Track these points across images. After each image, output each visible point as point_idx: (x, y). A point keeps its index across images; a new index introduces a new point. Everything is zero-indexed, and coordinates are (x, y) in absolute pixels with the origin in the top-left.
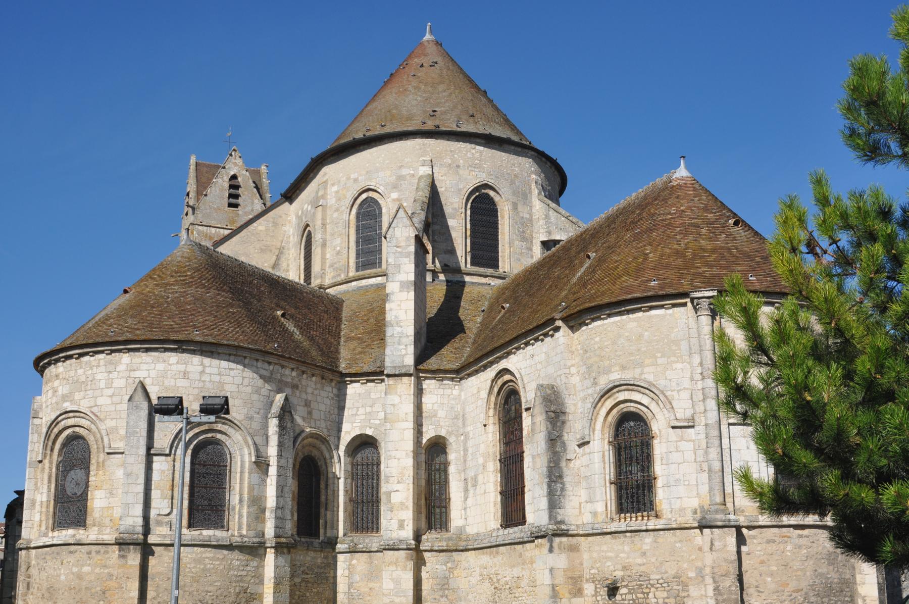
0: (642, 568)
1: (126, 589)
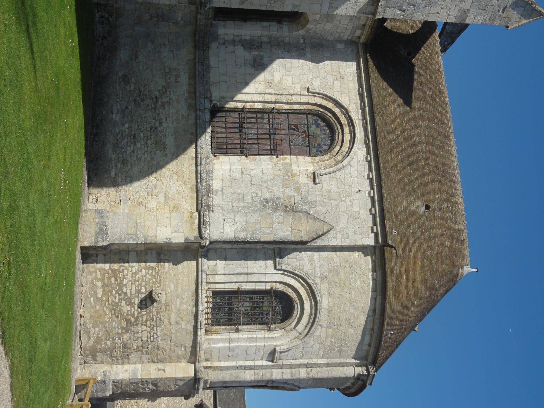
0: (166, 321)
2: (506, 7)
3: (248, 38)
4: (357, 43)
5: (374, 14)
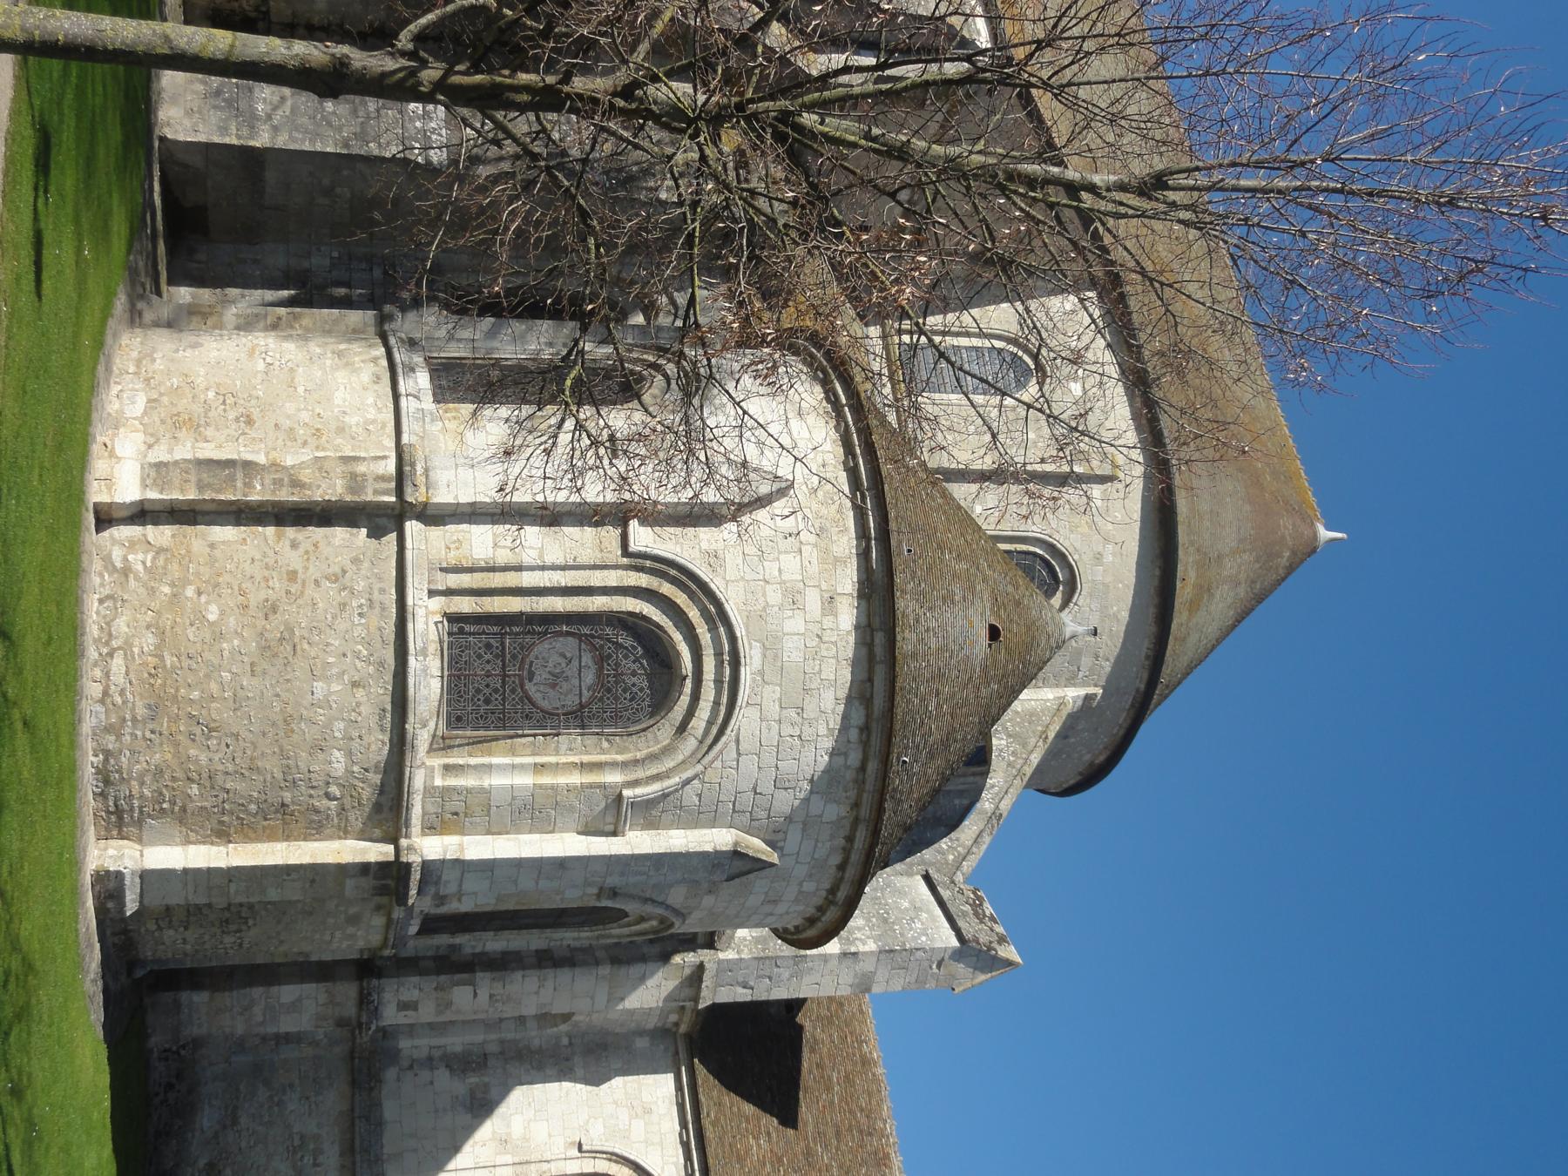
2: (943, 959)
3: (458, 1049)
4: (675, 1033)
5: (696, 999)
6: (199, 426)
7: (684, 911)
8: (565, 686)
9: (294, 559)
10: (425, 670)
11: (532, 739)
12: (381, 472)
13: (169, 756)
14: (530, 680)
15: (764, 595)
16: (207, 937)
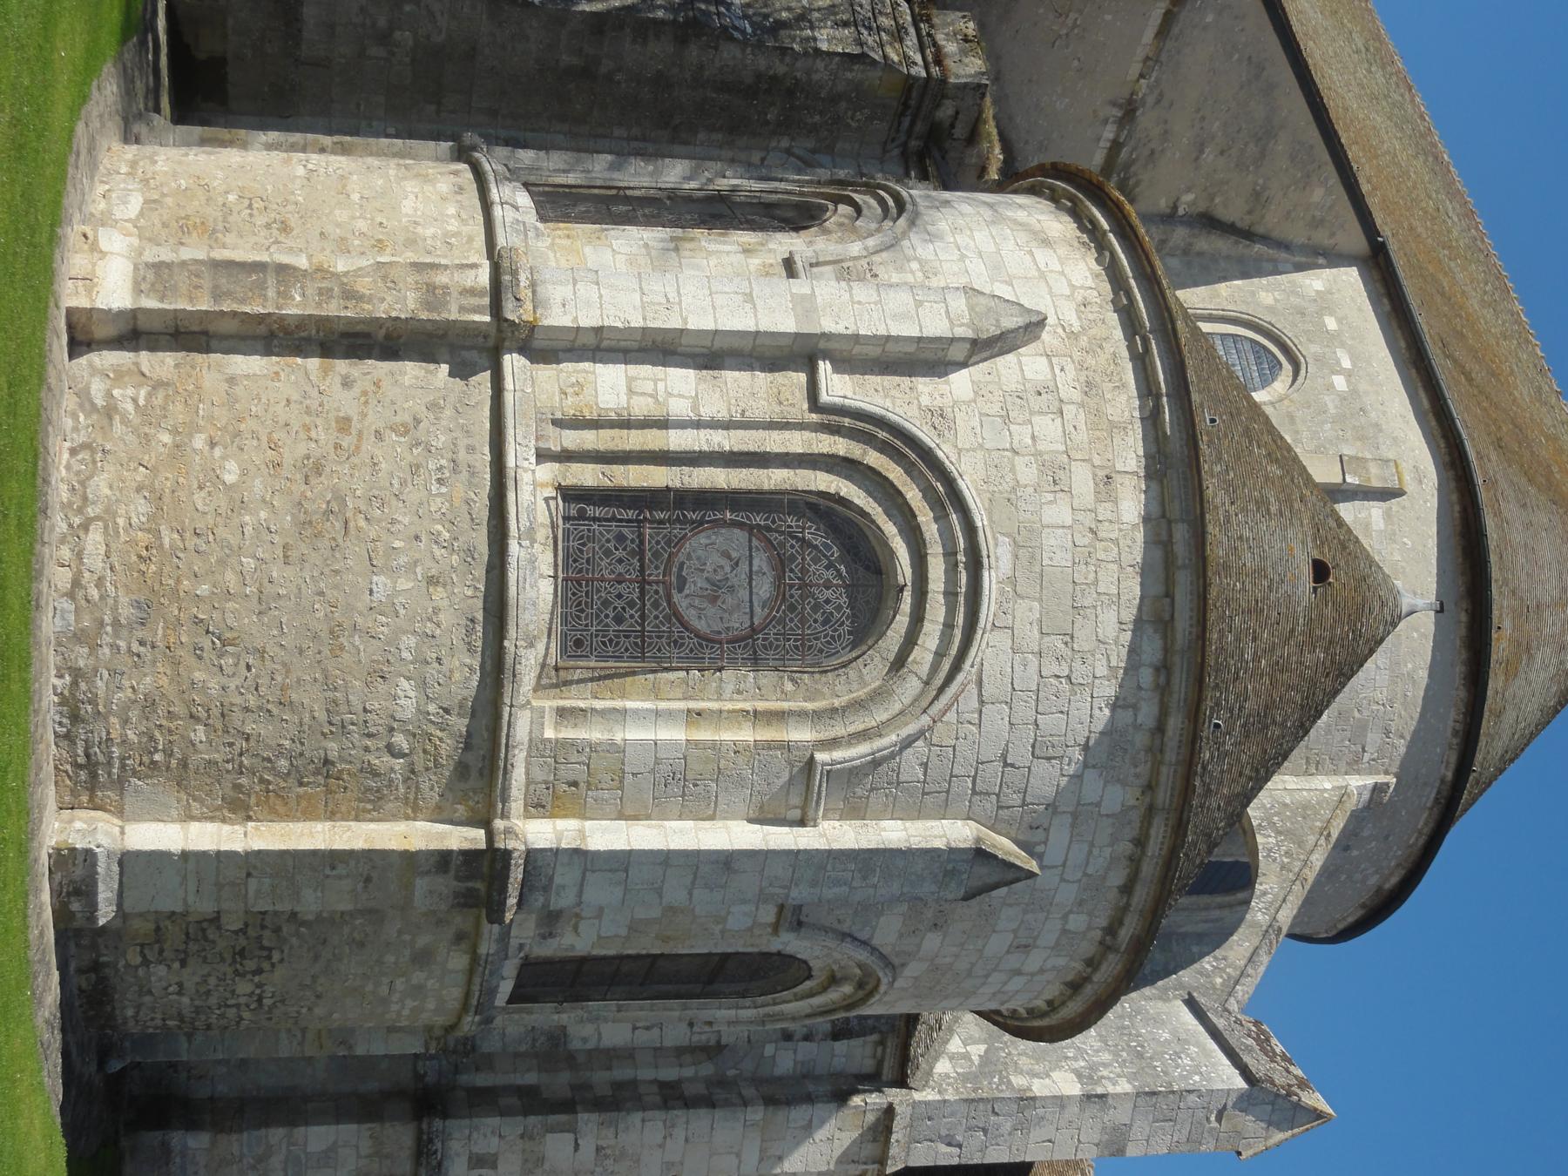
1: (328, 876)
2: (1225, 1107)
5: (882, 1161)
6: (214, 231)
7: (896, 961)
8: (730, 601)
9: (345, 402)
10: (532, 561)
11: (682, 674)
12: (469, 283)
13: (164, 681)
14: (680, 590)
15: (1013, 470)
16: (212, 981)
